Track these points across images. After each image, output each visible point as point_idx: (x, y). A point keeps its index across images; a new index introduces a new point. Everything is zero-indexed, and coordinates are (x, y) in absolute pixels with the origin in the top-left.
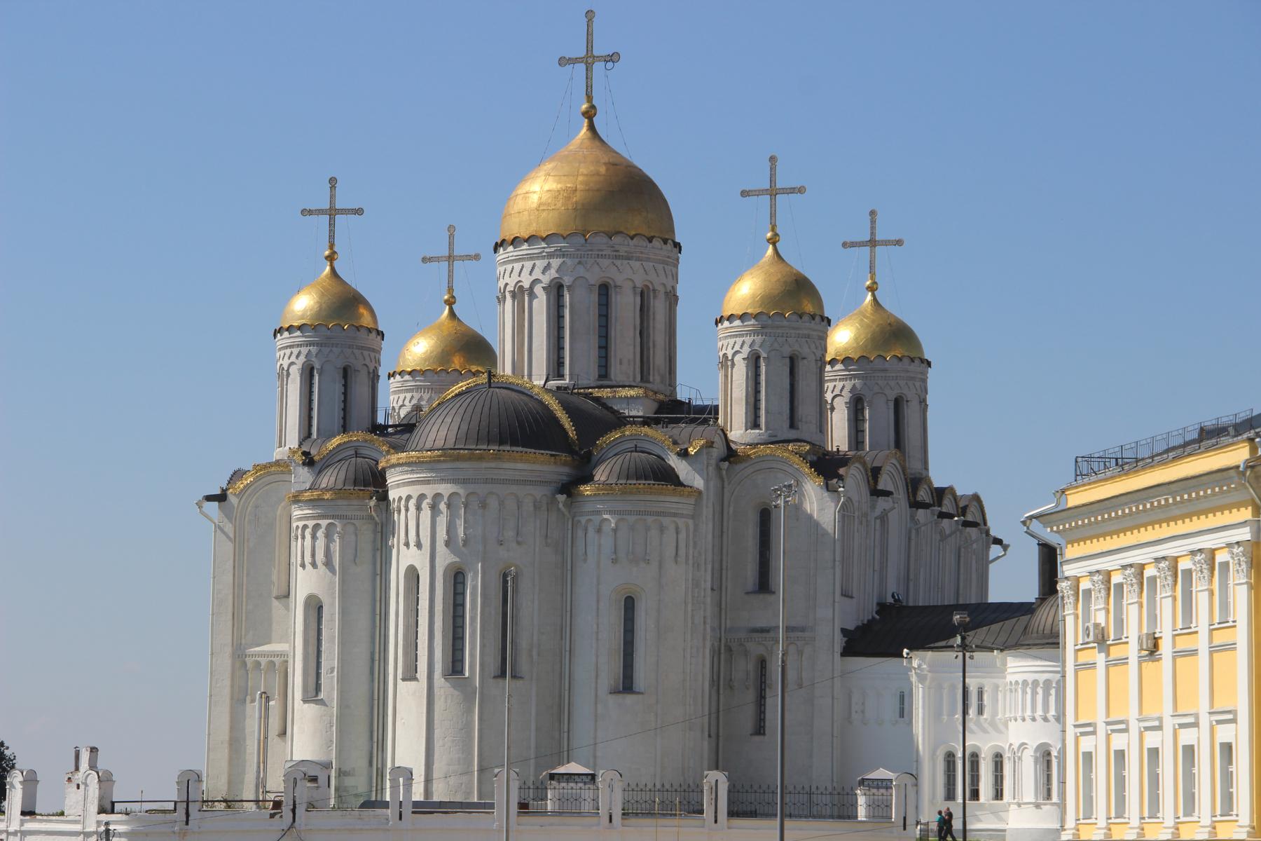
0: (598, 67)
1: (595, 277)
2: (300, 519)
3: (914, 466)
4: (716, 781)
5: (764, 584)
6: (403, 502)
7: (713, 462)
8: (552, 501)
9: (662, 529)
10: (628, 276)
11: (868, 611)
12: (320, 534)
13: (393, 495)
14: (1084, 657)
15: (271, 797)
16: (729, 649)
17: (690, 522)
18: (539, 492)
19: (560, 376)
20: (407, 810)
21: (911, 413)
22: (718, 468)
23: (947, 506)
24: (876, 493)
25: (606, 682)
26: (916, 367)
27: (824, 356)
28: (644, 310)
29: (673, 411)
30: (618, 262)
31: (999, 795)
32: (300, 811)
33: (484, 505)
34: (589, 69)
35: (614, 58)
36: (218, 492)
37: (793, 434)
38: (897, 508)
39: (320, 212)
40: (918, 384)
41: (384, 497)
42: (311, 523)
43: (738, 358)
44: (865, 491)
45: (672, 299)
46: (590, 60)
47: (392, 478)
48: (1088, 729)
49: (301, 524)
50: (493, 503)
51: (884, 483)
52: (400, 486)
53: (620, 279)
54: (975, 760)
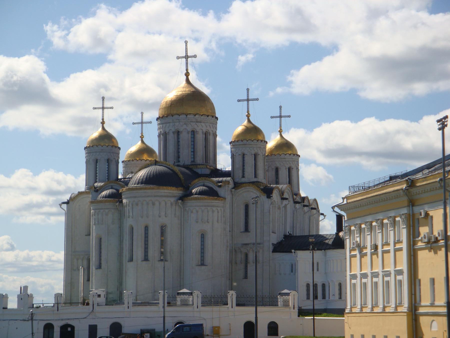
1: (190, 128)
3: (295, 190)
4: (232, 296)
5: (247, 229)
7: (230, 189)
8: (176, 203)
9: (213, 211)
10: (201, 128)
11: (281, 238)
14: (353, 253)
16: (236, 251)
17: (222, 209)
18: (173, 200)
19: (179, 161)
20: (131, 304)
21: (294, 172)
22: (231, 191)
23: (306, 203)
26: (295, 157)
28: (206, 139)
30: (197, 124)
31: (324, 297)
32: (95, 306)
33: (154, 204)
34: (187, 60)
36: (66, 201)
37: (255, 180)
38: (290, 204)
40: (296, 163)
41: (121, 202)
45: (215, 136)
48: (354, 277)
50: (157, 203)
51: (286, 196)
54: (315, 286)
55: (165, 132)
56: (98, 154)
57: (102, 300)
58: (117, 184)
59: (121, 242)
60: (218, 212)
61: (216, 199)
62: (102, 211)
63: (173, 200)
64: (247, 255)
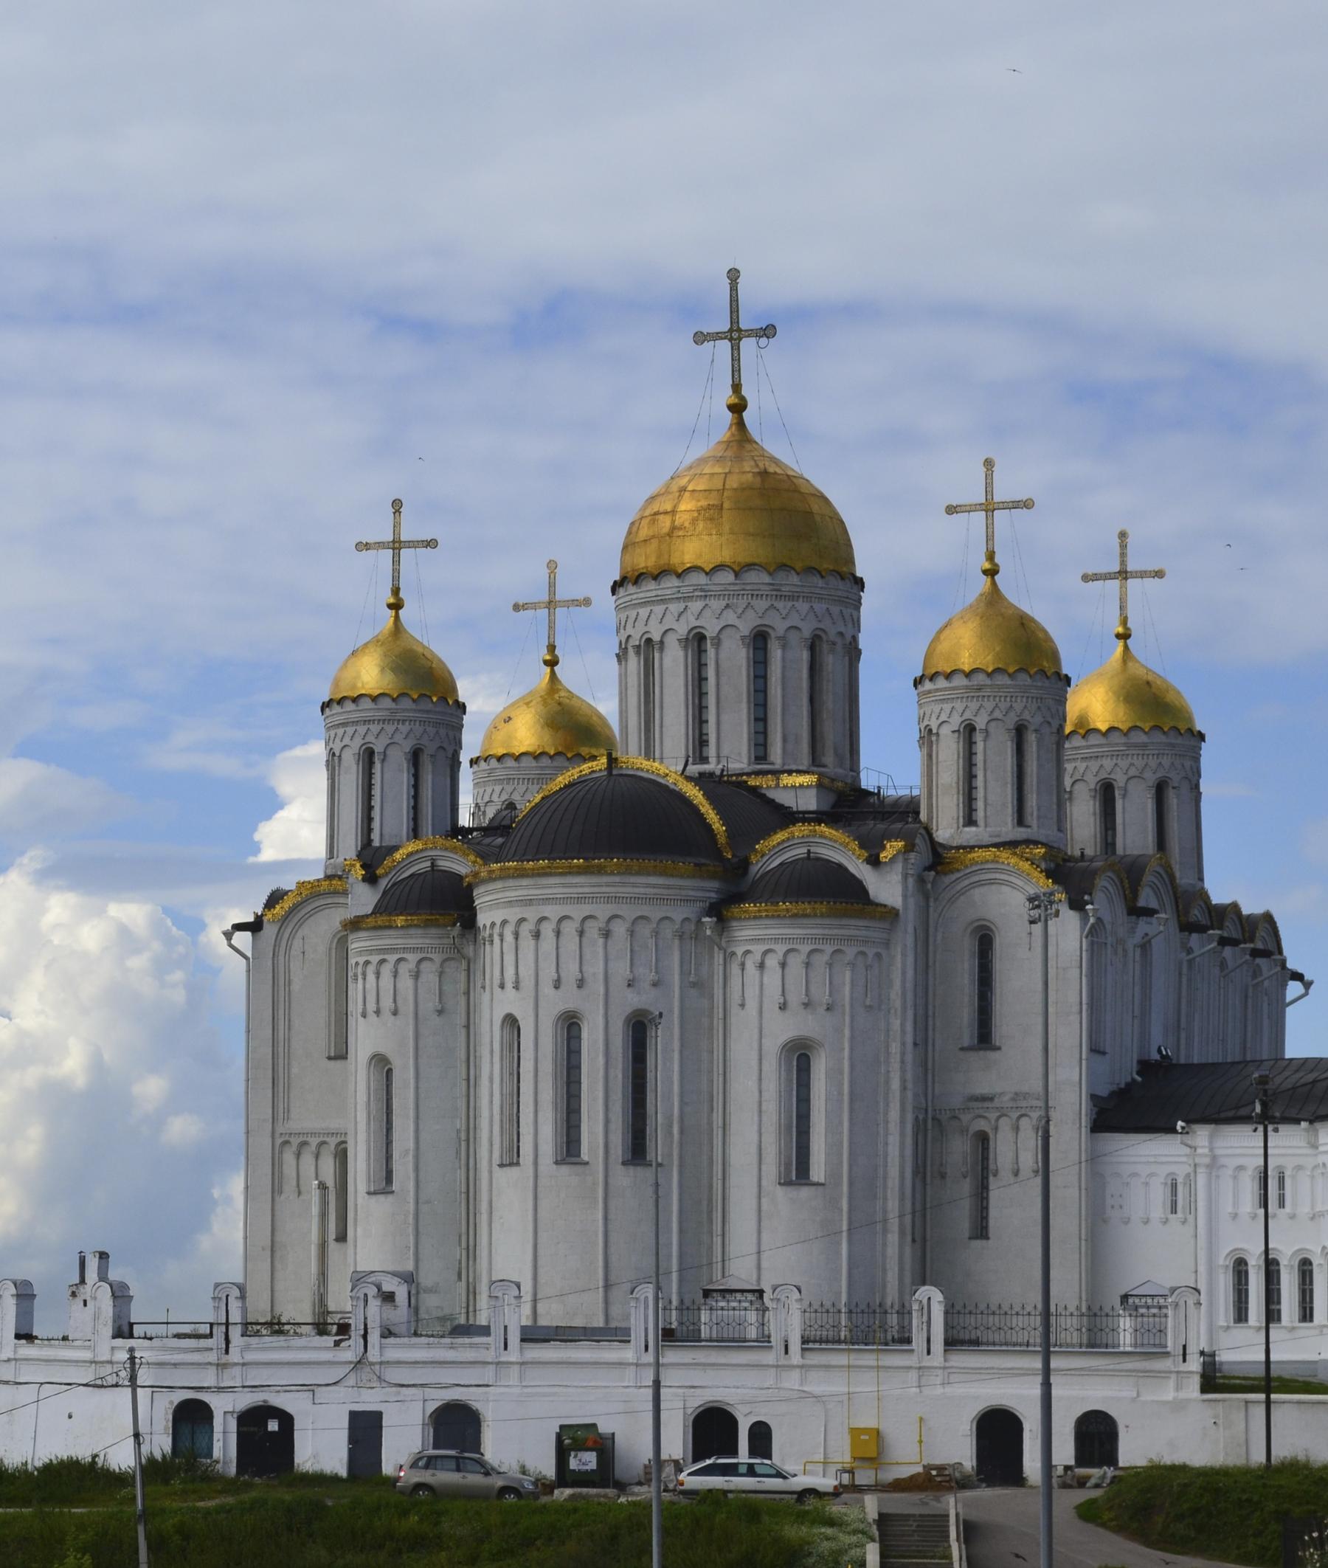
0: (747, 345)
2: (360, 953)
3: (1184, 879)
6: (497, 930)
11: (1128, 1072)
12: (387, 970)
13: (483, 919)
15: (336, 1318)
17: (884, 953)
18: (679, 913)
19: (704, 760)
22: (921, 881)
24: (1137, 912)
25: (771, 1169)
27: (1061, 727)
28: (815, 668)
29: (851, 806)
30: (780, 605)
31: (1306, 1314)
32: (374, 1337)
34: (736, 349)
35: (769, 332)
36: (251, 919)
37: (1021, 833)
39: (381, 545)
41: (469, 923)
42: (375, 959)
43: (945, 731)
44: (1120, 909)
45: (853, 653)
46: (735, 335)
47: (482, 897)
49: (361, 960)
51: (1146, 898)
52: (492, 907)
53: (779, 626)
54: (1271, 1269)
55: (649, 641)
56: (375, 728)
57: (400, 1313)
58: (454, 850)
59: (471, 1083)
60: (868, 967)
61: (860, 915)
62: (392, 958)
63: (679, 913)
64: (983, 1140)
